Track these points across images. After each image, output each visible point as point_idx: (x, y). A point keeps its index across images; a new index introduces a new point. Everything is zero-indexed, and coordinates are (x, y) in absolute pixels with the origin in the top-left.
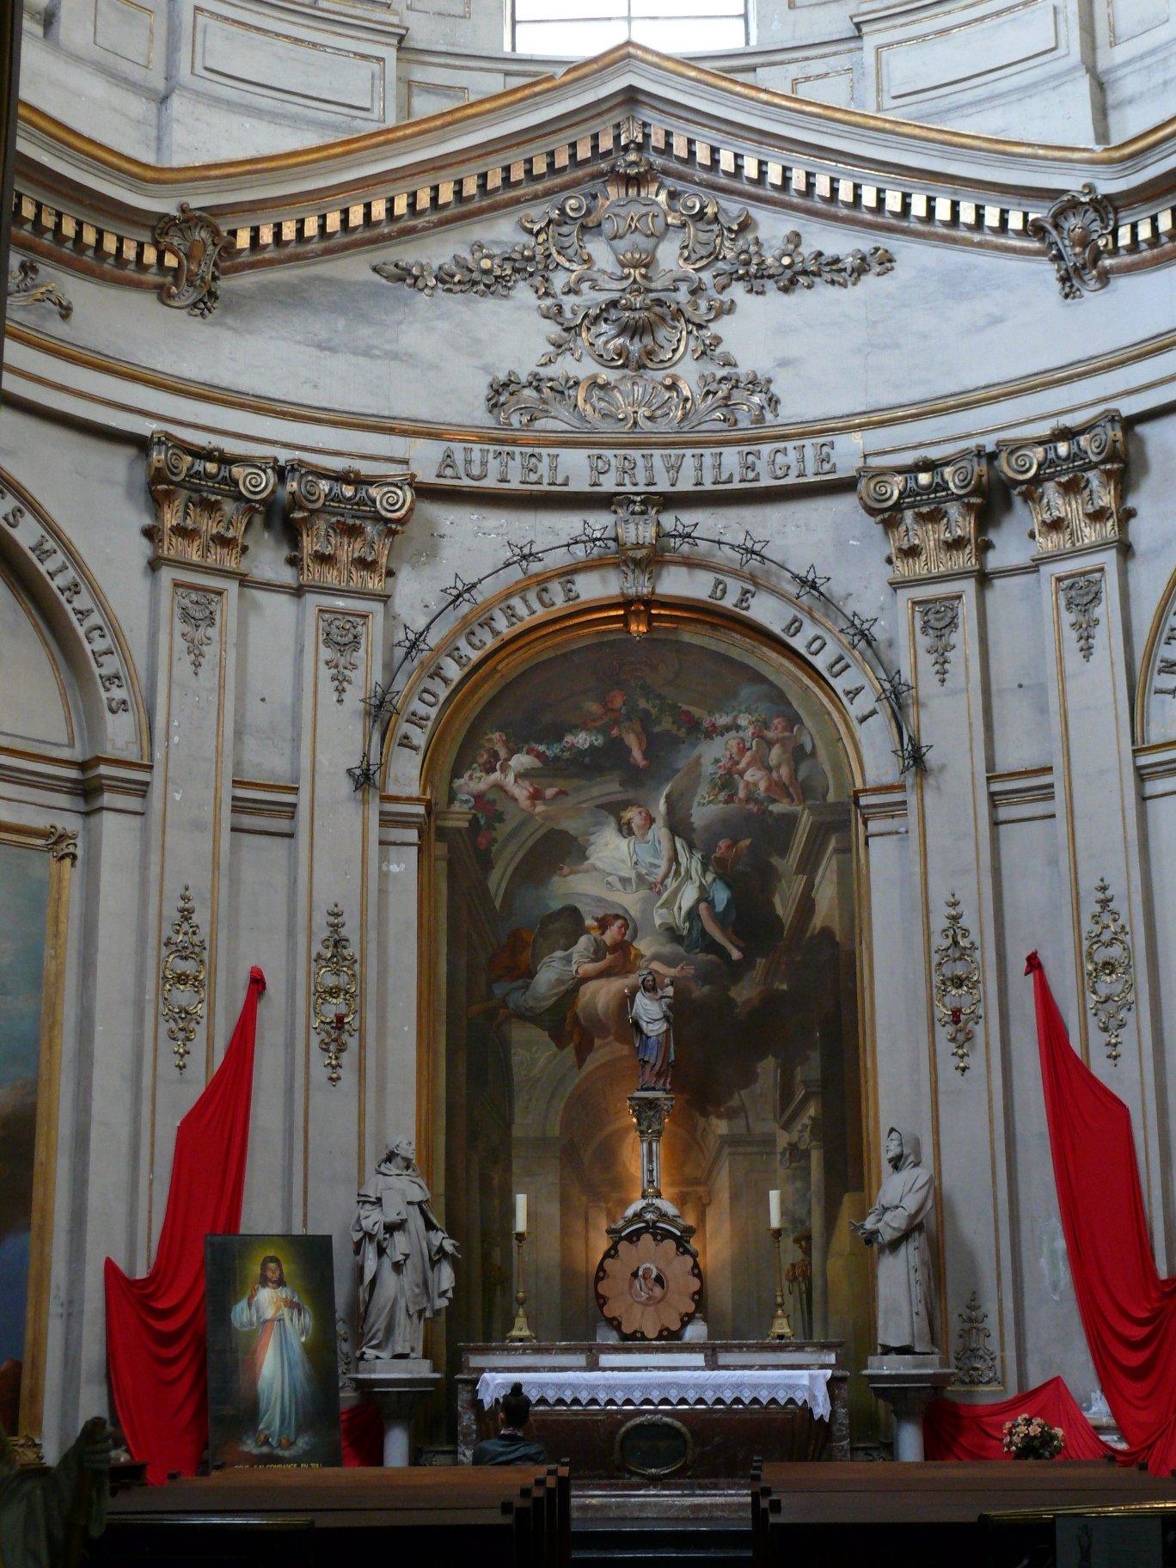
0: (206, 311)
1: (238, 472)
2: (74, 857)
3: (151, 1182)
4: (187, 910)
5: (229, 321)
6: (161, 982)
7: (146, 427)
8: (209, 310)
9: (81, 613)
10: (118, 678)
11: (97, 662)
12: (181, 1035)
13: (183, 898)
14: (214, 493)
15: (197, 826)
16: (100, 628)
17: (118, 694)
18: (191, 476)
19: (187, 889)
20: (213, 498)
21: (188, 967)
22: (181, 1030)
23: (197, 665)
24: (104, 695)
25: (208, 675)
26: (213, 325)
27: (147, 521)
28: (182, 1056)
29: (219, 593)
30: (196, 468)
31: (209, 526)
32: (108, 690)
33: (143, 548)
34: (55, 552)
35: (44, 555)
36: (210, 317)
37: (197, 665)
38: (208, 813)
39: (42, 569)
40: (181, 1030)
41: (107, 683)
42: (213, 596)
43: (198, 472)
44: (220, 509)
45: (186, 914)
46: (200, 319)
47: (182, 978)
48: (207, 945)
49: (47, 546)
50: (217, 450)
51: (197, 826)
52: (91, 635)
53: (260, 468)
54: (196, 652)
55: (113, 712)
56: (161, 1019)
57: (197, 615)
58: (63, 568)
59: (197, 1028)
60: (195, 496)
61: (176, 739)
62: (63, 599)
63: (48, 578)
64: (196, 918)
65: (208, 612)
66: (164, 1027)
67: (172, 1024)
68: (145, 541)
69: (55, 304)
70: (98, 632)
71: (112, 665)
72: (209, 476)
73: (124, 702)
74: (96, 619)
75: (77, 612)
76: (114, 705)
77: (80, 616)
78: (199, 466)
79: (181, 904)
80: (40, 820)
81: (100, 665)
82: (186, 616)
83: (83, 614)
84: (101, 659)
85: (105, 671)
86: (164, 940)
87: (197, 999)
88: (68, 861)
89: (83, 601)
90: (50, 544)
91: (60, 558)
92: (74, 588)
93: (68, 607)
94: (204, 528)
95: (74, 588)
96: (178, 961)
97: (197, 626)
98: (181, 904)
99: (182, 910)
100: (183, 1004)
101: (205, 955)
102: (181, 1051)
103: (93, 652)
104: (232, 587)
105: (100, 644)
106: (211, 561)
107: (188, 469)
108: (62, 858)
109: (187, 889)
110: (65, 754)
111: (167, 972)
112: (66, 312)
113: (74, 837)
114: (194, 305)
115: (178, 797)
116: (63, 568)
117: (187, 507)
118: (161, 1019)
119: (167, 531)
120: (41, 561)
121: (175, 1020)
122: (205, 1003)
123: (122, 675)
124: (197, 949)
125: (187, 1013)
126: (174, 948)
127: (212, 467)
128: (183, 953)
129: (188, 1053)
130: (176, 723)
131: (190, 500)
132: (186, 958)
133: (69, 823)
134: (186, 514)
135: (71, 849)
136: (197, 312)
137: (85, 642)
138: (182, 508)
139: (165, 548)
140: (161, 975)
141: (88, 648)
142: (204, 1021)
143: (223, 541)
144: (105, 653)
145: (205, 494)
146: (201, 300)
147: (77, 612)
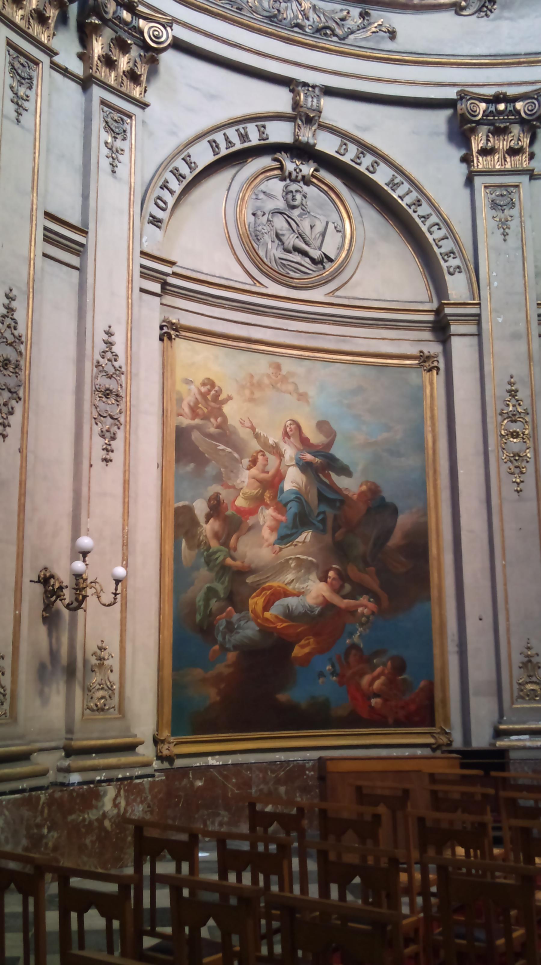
0: (489, 13)
1: (519, 105)
2: (438, 369)
3: (504, 566)
4: (513, 391)
5: (506, 14)
6: (499, 438)
7: (451, 93)
8: (491, 12)
9: (424, 217)
10: (453, 253)
11: (437, 245)
12: (517, 471)
13: (510, 383)
14: (502, 123)
15: (515, 336)
16: (437, 224)
17: (454, 262)
18: (487, 116)
19: (512, 377)
20: (502, 126)
21: (515, 427)
22: (516, 467)
23: (505, 235)
24: (444, 265)
25: (513, 241)
26: (494, 19)
27: (463, 152)
28: (518, 484)
29: (517, 186)
30: (490, 109)
31: (502, 144)
32: (446, 261)
33: (463, 168)
34: (403, 183)
35: (394, 186)
36: (492, 16)
37: (505, 235)
38: (522, 326)
39: (395, 196)
40: (516, 467)
41: (446, 257)
42: (512, 189)
43: (492, 112)
44: (511, 133)
45: (513, 393)
46: (485, 18)
47: (515, 435)
48: (530, 411)
49: (396, 181)
50: (501, 93)
51: (515, 336)
52: (432, 230)
53: (534, 98)
54: (504, 225)
55: (451, 274)
56: (501, 462)
57: (502, 203)
58: (408, 192)
59: (528, 465)
60: (492, 128)
61: (496, 284)
62: (410, 211)
63: (400, 201)
64: (519, 396)
65: (509, 199)
66: (504, 468)
67: (509, 464)
68: (464, 166)
69: (385, 32)
70: (437, 227)
71: (448, 245)
72: (501, 113)
73: (459, 267)
74: (434, 219)
75: (420, 217)
76: (451, 270)
77: (423, 219)
78: (492, 108)
79: (509, 387)
80: (413, 350)
81: (440, 247)
82: (494, 205)
83: (425, 218)
84: (440, 243)
85: (443, 250)
86: (499, 411)
87: (524, 447)
88: (435, 372)
89: (425, 209)
90: (399, 179)
91: (406, 186)
92: (418, 203)
93: (415, 216)
94: (501, 147)
95: (418, 203)
96: (510, 423)
97: (503, 211)
98: (509, 387)
99: (509, 391)
100: (516, 450)
101: (528, 418)
102: (518, 480)
103: (434, 240)
104: (525, 179)
105: (438, 234)
106: (508, 166)
107: (484, 112)
108: (430, 370)
109: (512, 377)
110: (427, 307)
111: (503, 432)
112: (392, 34)
113: (437, 356)
114: (480, 10)
115: (500, 320)
116: (408, 192)
117: (488, 136)
118: (501, 462)
119: (475, 154)
120: (394, 190)
121: (511, 461)
122: (532, 449)
123: (455, 250)
124: (522, 415)
125: (519, 456)
126: (506, 416)
127: (502, 107)
128: (513, 418)
129: (522, 482)
130: (494, 274)
131: (489, 131)
132: (515, 421)
133: (435, 348)
134: (488, 140)
135: (435, 364)
136: (483, 14)
137: (428, 235)
138: (484, 138)
139: (476, 165)
140: (499, 433)
141: (430, 238)
142: (532, 461)
143: (513, 152)
144: (443, 239)
145: (497, 125)
146: (484, 6)
147: (420, 217)
